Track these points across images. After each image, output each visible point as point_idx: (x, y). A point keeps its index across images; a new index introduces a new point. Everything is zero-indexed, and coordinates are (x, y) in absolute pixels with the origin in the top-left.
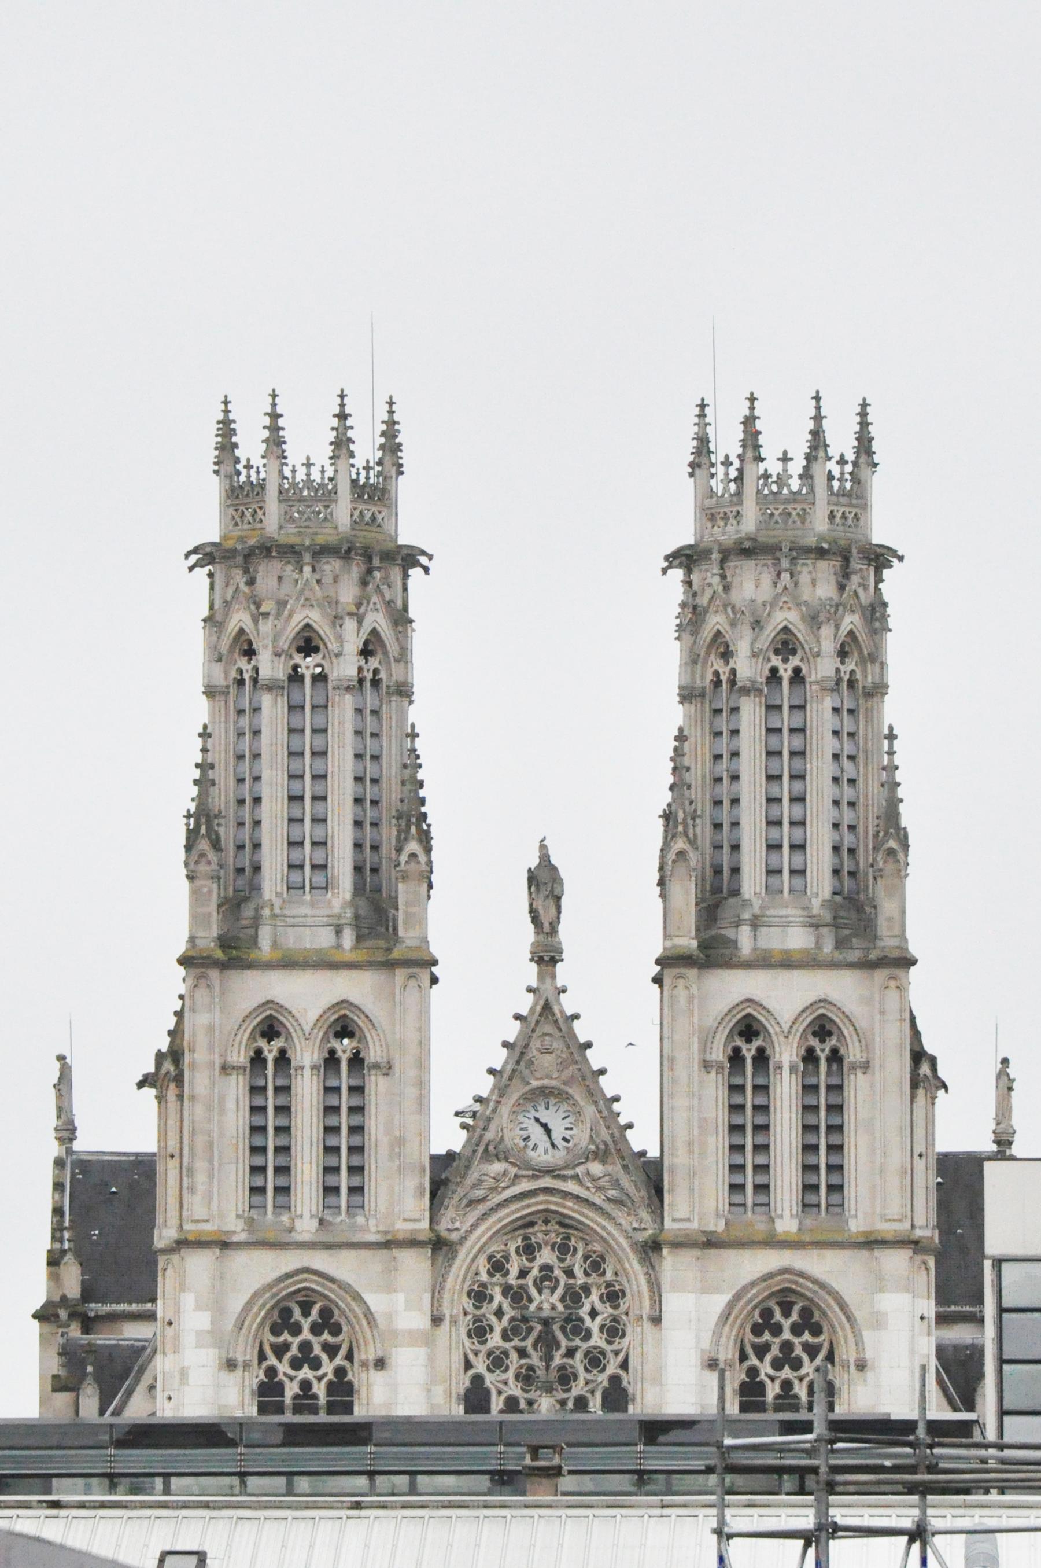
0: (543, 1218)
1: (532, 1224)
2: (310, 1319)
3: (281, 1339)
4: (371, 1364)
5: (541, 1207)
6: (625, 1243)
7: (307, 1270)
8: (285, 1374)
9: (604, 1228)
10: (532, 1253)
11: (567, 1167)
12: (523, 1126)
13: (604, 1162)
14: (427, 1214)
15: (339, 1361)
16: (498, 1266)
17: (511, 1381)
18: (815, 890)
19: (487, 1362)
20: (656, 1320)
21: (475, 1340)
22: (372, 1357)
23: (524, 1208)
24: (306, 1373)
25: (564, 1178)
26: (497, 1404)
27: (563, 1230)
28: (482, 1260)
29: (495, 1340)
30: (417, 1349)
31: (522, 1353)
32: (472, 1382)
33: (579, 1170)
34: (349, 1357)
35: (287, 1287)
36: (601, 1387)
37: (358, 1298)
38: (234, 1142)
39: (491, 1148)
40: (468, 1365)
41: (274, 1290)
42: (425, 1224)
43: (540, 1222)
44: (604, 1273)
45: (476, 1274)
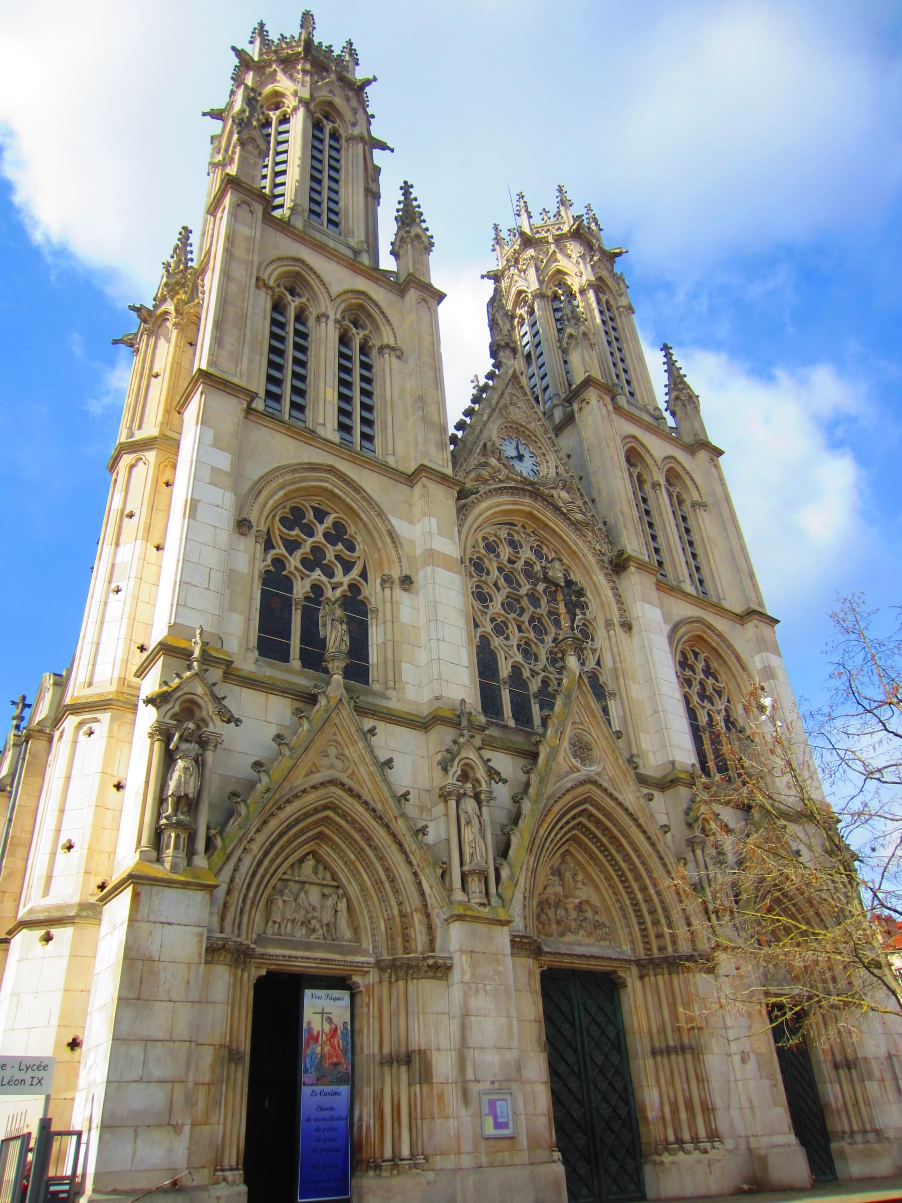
2: (325, 525)
3: (294, 533)
4: (397, 582)
5: (528, 509)
6: (592, 560)
7: (332, 470)
8: (296, 568)
9: (576, 544)
15: (355, 573)
16: (491, 548)
20: (627, 626)
22: (396, 574)
23: (515, 503)
24: (317, 574)
29: (496, 607)
34: (364, 575)
35: (306, 480)
37: (381, 514)
38: (260, 338)
41: (296, 475)
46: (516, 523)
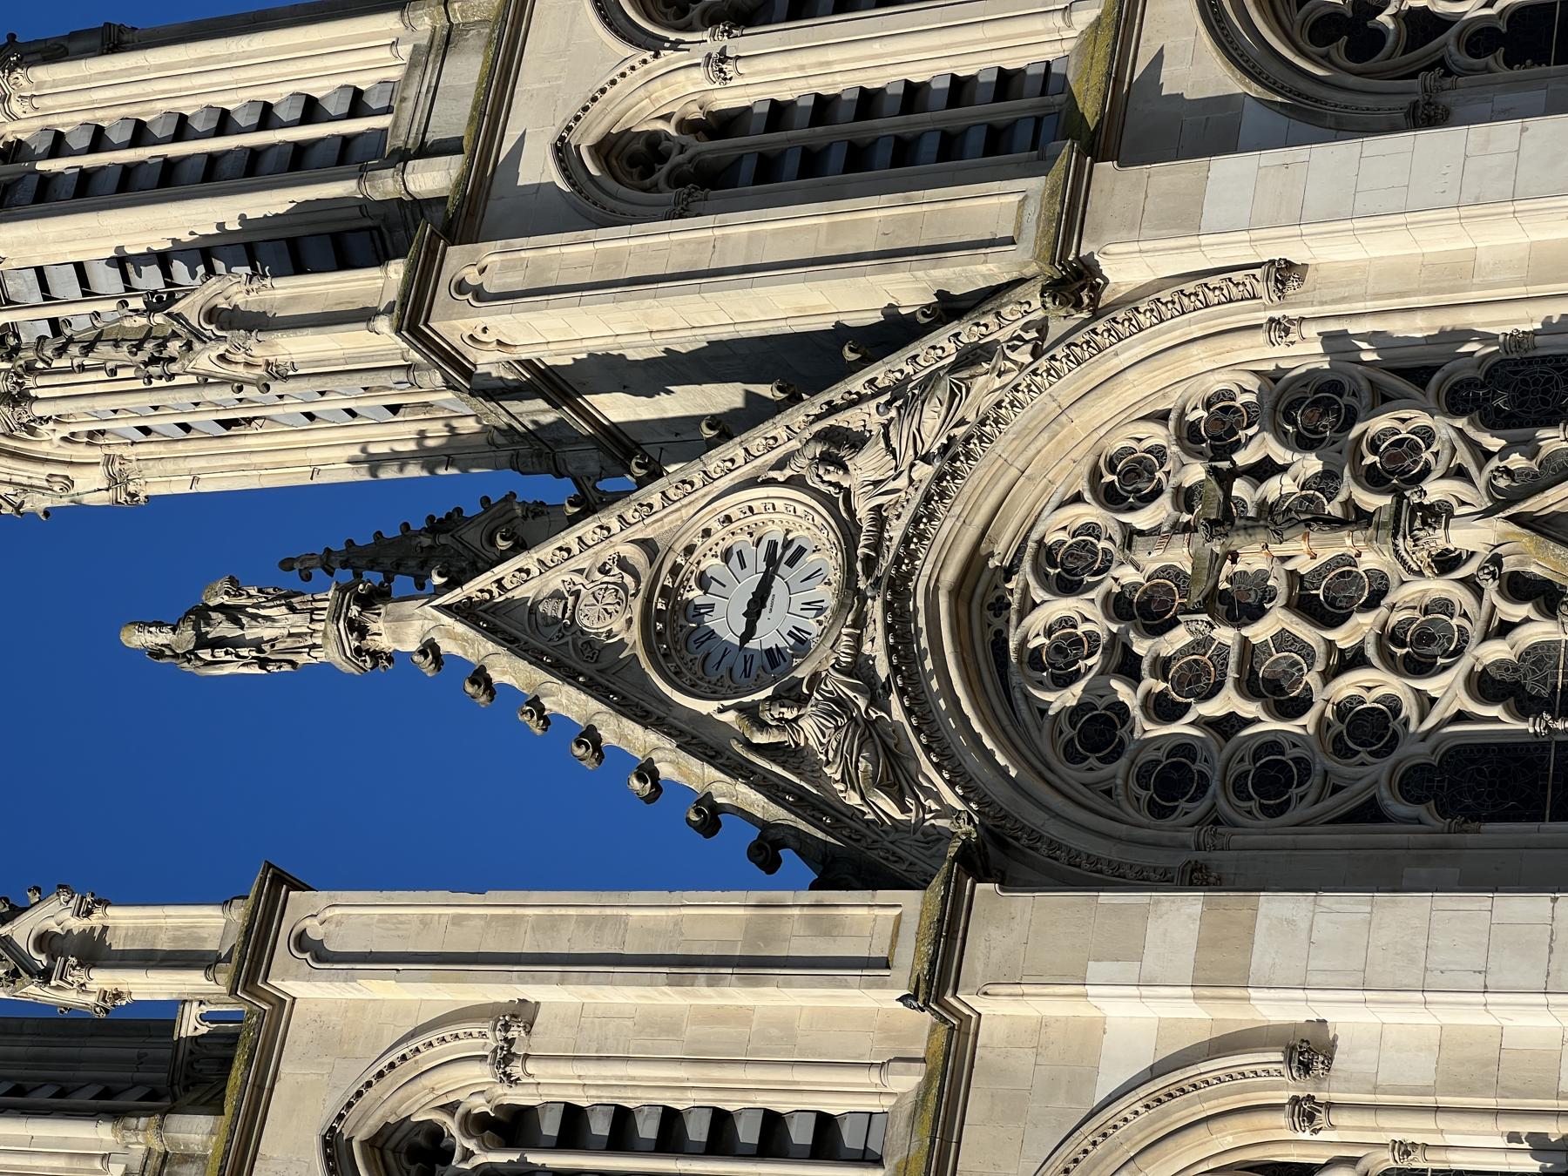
0: (990, 614)
1: (1000, 642)
10: (1079, 642)
11: (848, 530)
12: (739, 669)
13: (857, 441)
14: (884, 896)
17: (1431, 686)
18: (385, 53)
19: (1363, 756)
21: (1294, 792)
25: (877, 545)
26: (1496, 720)
27: (1027, 565)
28: (1073, 774)
30: (1262, 924)
31: (1353, 660)
32: (1418, 801)
33: (863, 510)
36: (1472, 432)
39: (760, 738)
40: (1370, 812)
42: (910, 900)
43: (998, 623)
44: (1159, 452)
45: (1108, 792)
46: (990, 637)
